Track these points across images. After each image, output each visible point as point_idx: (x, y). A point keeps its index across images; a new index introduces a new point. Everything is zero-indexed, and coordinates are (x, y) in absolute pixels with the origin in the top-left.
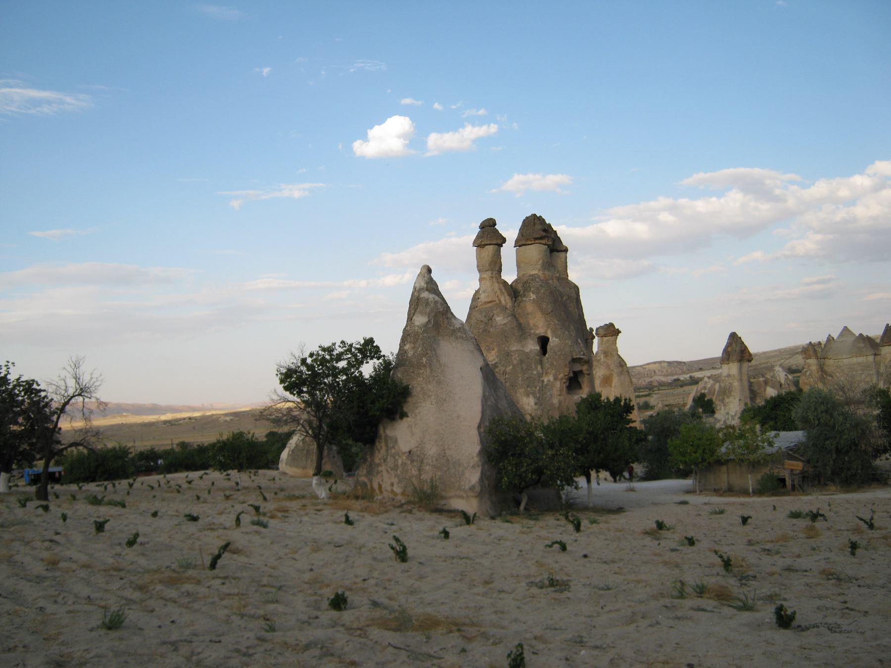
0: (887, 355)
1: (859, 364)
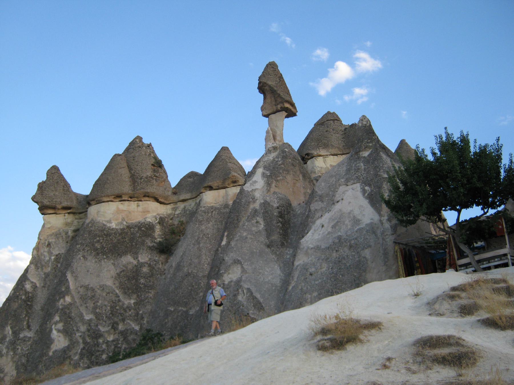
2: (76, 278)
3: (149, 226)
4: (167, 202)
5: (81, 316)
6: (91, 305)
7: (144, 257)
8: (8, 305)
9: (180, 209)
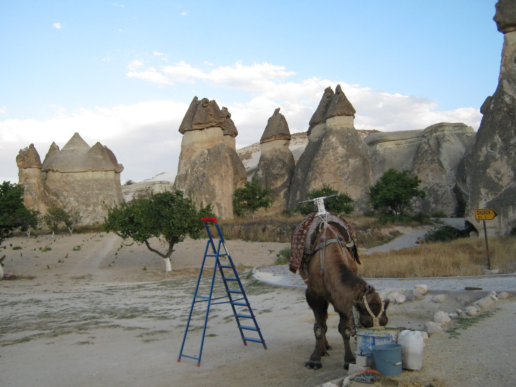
0: (196, 145)
1: (96, 180)
8: (492, 117)
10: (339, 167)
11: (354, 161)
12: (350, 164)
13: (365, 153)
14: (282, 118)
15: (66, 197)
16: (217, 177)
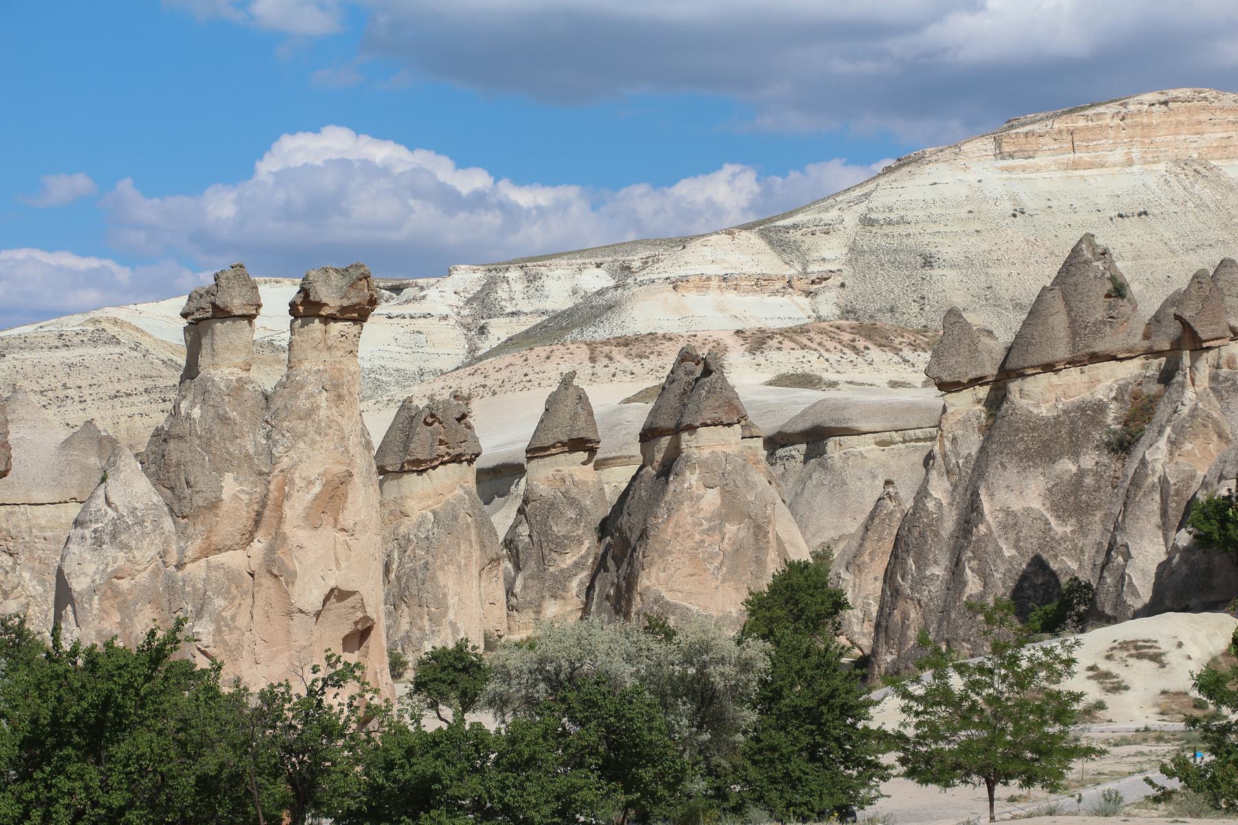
2: (992, 495)
3: (1099, 406)
4: (1133, 355)
5: (998, 552)
6: (1012, 536)
7: (1089, 460)
9: (1154, 368)
10: (703, 541)
11: (735, 528)
12: (727, 536)
13: (760, 513)
14: (580, 398)
15: (7, 569)
16: (452, 569)
